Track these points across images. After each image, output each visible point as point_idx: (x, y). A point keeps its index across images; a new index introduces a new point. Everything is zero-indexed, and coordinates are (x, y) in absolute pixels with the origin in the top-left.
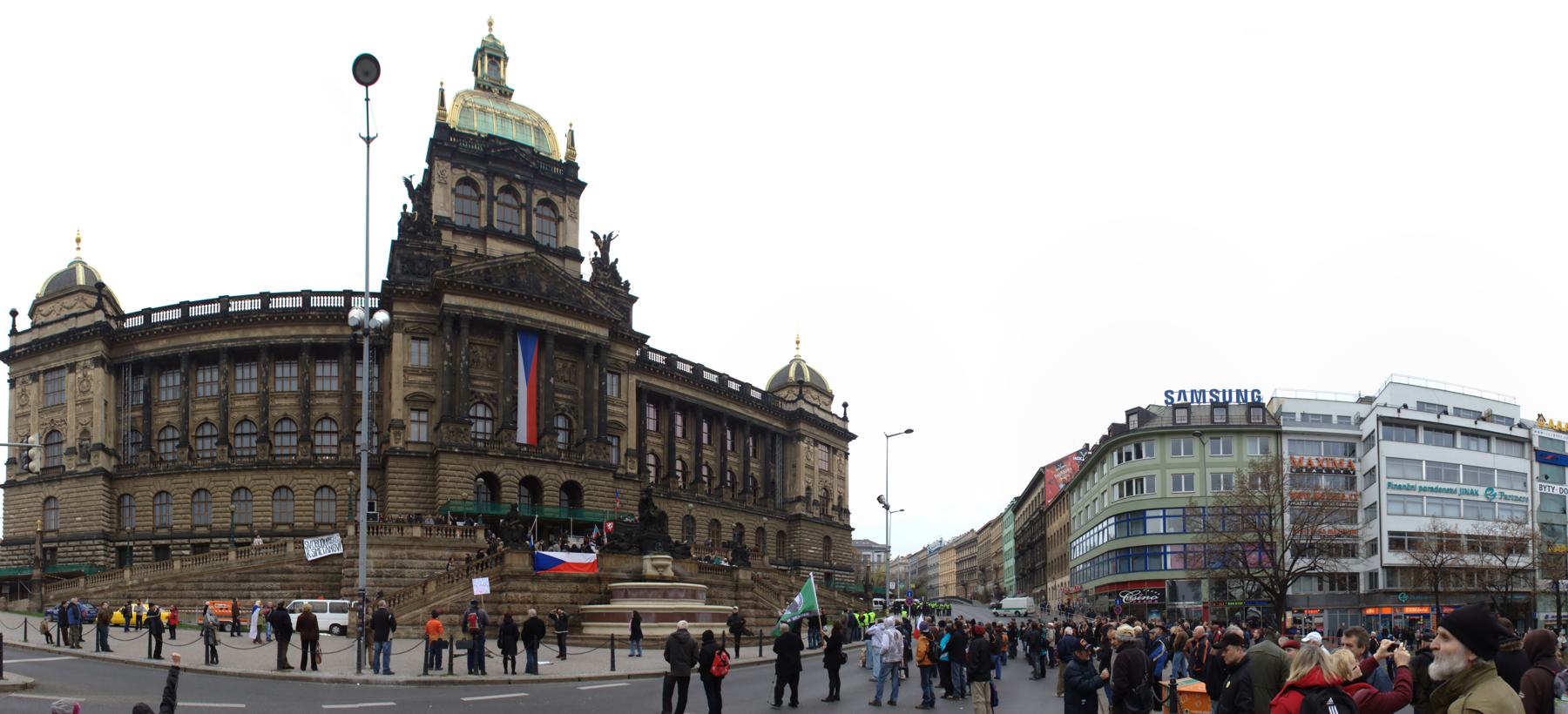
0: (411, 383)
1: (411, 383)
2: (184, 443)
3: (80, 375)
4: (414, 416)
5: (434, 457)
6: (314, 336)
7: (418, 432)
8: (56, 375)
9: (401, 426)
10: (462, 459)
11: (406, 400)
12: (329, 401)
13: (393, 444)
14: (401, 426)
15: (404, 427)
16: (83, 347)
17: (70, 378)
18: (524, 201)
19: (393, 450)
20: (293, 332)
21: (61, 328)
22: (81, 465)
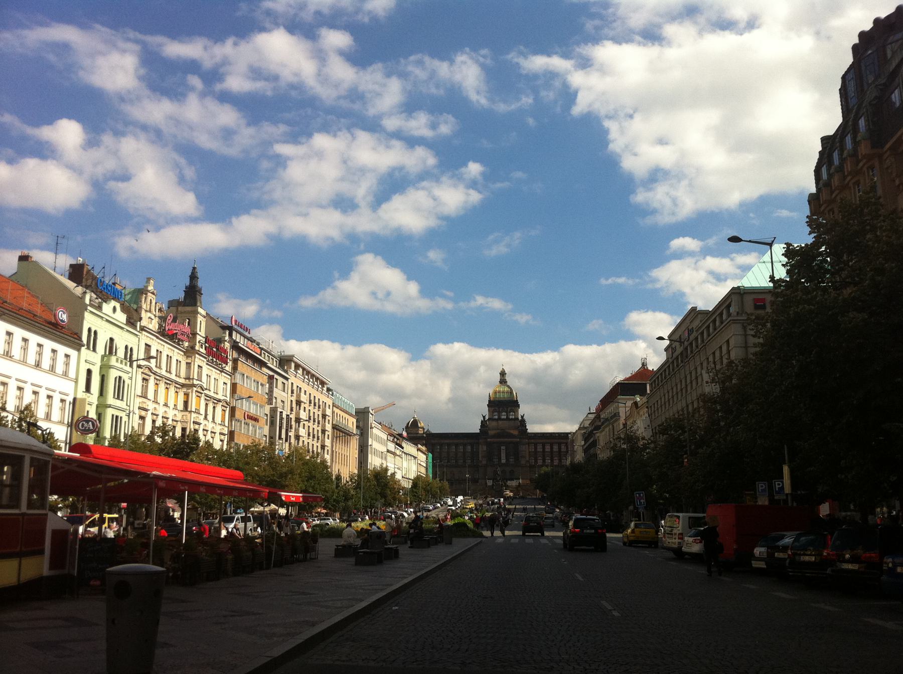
7: (484, 462)
9: (481, 462)
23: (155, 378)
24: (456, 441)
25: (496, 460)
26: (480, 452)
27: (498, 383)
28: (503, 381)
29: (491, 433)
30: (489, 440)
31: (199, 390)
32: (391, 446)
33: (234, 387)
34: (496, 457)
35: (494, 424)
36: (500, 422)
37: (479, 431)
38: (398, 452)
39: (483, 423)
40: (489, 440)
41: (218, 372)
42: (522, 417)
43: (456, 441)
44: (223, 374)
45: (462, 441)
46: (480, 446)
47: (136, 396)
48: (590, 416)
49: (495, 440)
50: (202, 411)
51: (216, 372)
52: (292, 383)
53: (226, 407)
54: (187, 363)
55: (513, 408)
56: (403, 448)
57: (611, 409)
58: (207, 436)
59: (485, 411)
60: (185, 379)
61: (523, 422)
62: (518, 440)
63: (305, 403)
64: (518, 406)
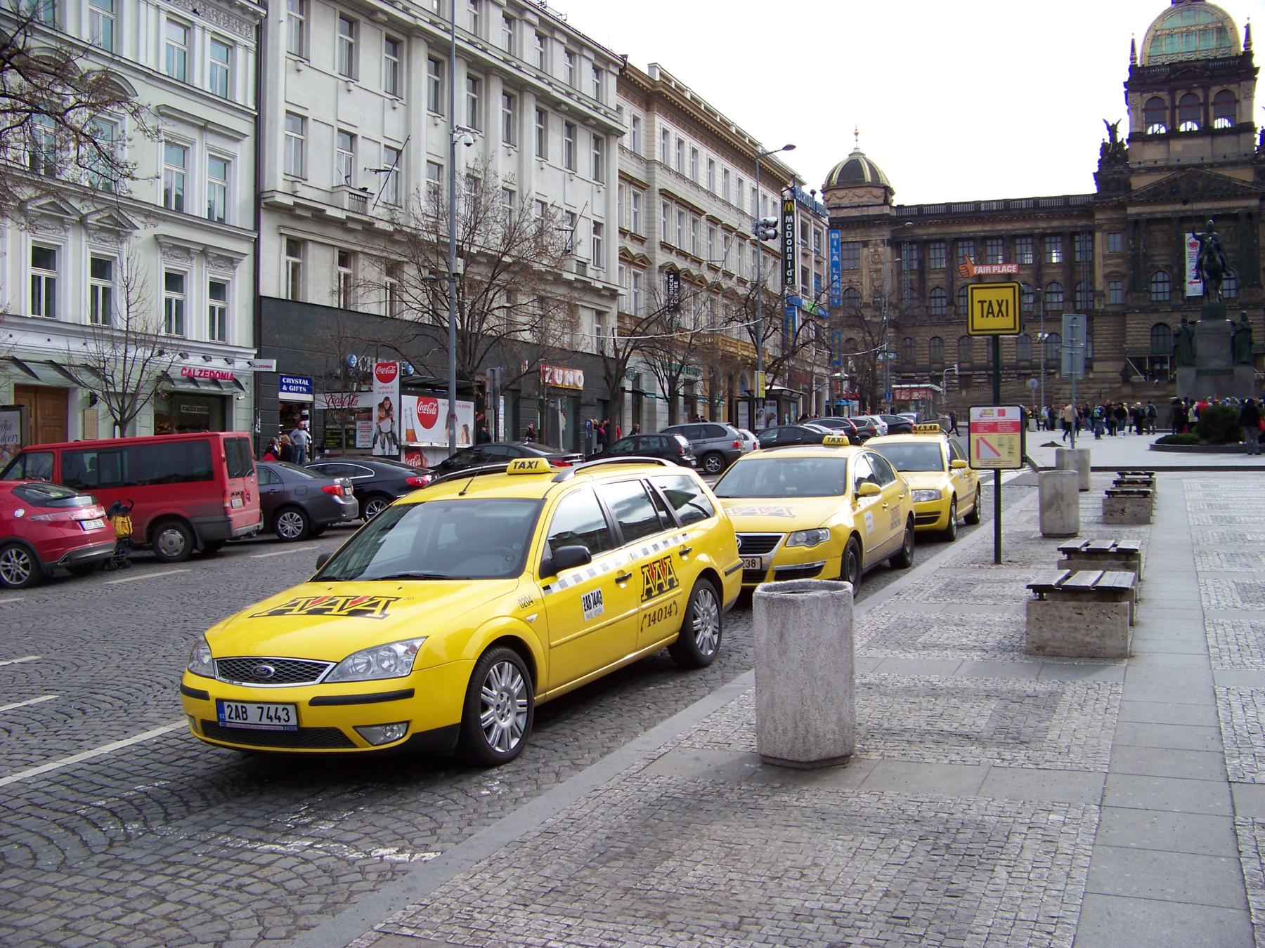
0: (1108, 265)
1: (1108, 265)
2: (951, 303)
3: (872, 250)
4: (1112, 285)
5: (1124, 314)
6: (1043, 228)
7: (1115, 296)
8: (851, 246)
10: (1142, 316)
11: (1105, 276)
12: (1055, 271)
13: (1097, 307)
14: (1102, 294)
15: (1104, 296)
16: (874, 230)
17: (865, 251)
18: (1202, 100)
19: (1097, 312)
20: (1028, 226)
21: (855, 213)
22: (875, 316)
24: (1003, 227)
25: (1160, 290)
26: (1098, 261)
29: (1138, 183)
30: (1131, 210)
34: (1160, 276)
36: (1177, 146)
37: (1091, 188)
39: (1112, 155)
40: (1131, 210)
43: (1003, 227)
45: (1028, 226)
46: (1098, 235)
49: (1159, 210)
55: (1232, 87)
62: (1254, 203)
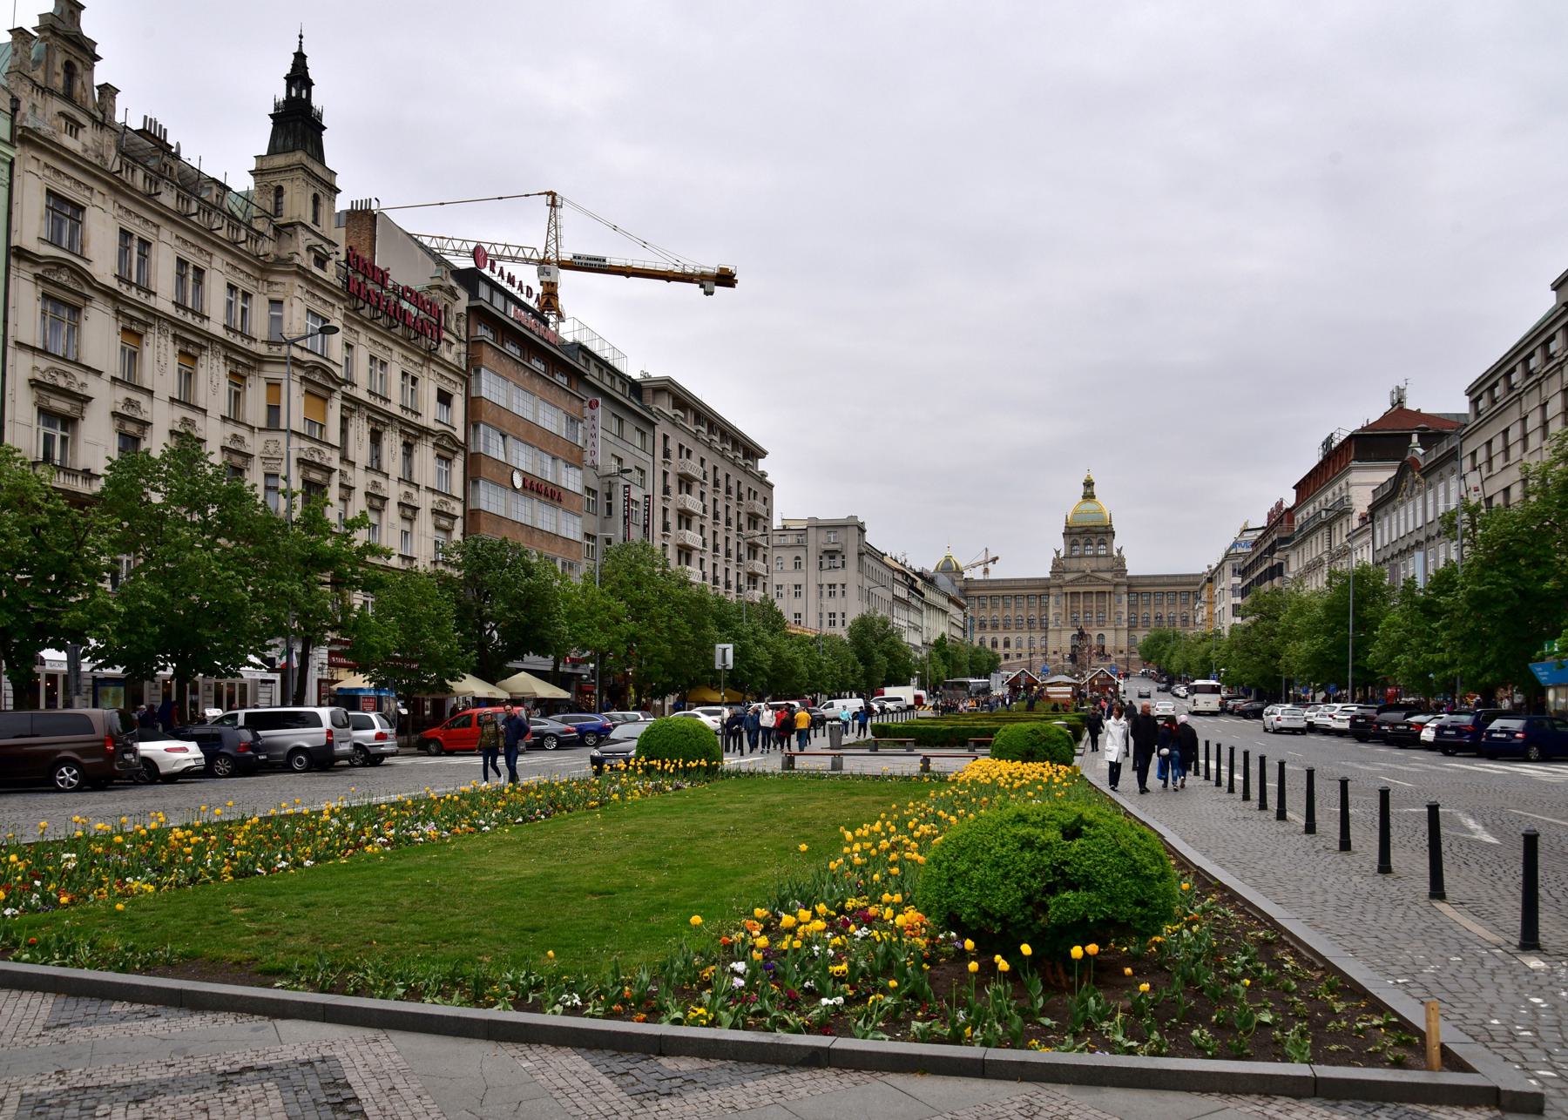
23: (118, 312)
27: (1081, 500)
28: (1089, 496)
29: (1069, 577)
31: (317, 377)
32: (902, 592)
33: (474, 406)
35: (1074, 564)
37: (1048, 576)
38: (914, 602)
41: (416, 359)
42: (1119, 551)
44: (433, 366)
47: (10, 343)
48: (1246, 534)
50: (334, 436)
51: (406, 358)
52: (666, 438)
53: (456, 453)
54: (271, 301)
56: (923, 595)
57: (1329, 496)
58: (350, 505)
59: (1060, 544)
60: (269, 343)
61: (1121, 561)
63: (702, 483)
64: (1113, 534)
